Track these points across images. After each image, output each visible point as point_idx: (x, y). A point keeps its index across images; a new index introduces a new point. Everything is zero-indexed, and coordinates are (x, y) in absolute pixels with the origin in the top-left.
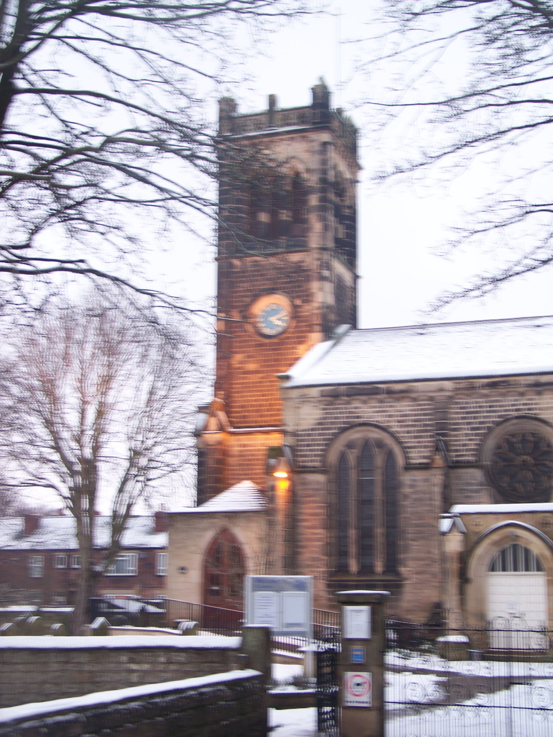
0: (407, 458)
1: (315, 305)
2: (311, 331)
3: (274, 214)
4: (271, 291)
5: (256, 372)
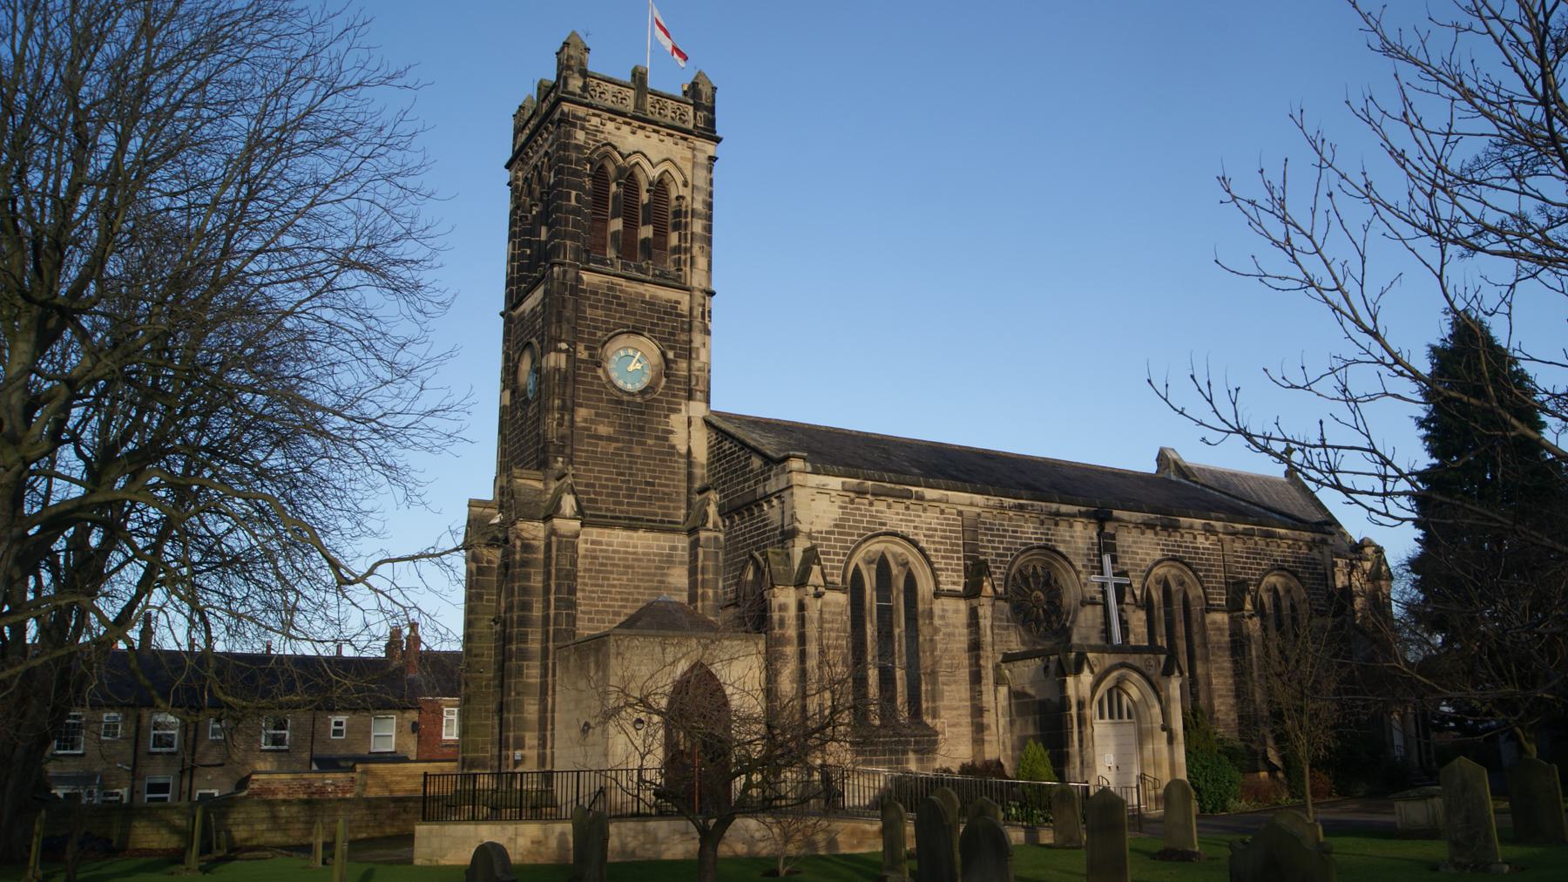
0: (937, 583)
1: (696, 364)
2: (690, 397)
3: (631, 225)
4: (636, 331)
5: (609, 439)
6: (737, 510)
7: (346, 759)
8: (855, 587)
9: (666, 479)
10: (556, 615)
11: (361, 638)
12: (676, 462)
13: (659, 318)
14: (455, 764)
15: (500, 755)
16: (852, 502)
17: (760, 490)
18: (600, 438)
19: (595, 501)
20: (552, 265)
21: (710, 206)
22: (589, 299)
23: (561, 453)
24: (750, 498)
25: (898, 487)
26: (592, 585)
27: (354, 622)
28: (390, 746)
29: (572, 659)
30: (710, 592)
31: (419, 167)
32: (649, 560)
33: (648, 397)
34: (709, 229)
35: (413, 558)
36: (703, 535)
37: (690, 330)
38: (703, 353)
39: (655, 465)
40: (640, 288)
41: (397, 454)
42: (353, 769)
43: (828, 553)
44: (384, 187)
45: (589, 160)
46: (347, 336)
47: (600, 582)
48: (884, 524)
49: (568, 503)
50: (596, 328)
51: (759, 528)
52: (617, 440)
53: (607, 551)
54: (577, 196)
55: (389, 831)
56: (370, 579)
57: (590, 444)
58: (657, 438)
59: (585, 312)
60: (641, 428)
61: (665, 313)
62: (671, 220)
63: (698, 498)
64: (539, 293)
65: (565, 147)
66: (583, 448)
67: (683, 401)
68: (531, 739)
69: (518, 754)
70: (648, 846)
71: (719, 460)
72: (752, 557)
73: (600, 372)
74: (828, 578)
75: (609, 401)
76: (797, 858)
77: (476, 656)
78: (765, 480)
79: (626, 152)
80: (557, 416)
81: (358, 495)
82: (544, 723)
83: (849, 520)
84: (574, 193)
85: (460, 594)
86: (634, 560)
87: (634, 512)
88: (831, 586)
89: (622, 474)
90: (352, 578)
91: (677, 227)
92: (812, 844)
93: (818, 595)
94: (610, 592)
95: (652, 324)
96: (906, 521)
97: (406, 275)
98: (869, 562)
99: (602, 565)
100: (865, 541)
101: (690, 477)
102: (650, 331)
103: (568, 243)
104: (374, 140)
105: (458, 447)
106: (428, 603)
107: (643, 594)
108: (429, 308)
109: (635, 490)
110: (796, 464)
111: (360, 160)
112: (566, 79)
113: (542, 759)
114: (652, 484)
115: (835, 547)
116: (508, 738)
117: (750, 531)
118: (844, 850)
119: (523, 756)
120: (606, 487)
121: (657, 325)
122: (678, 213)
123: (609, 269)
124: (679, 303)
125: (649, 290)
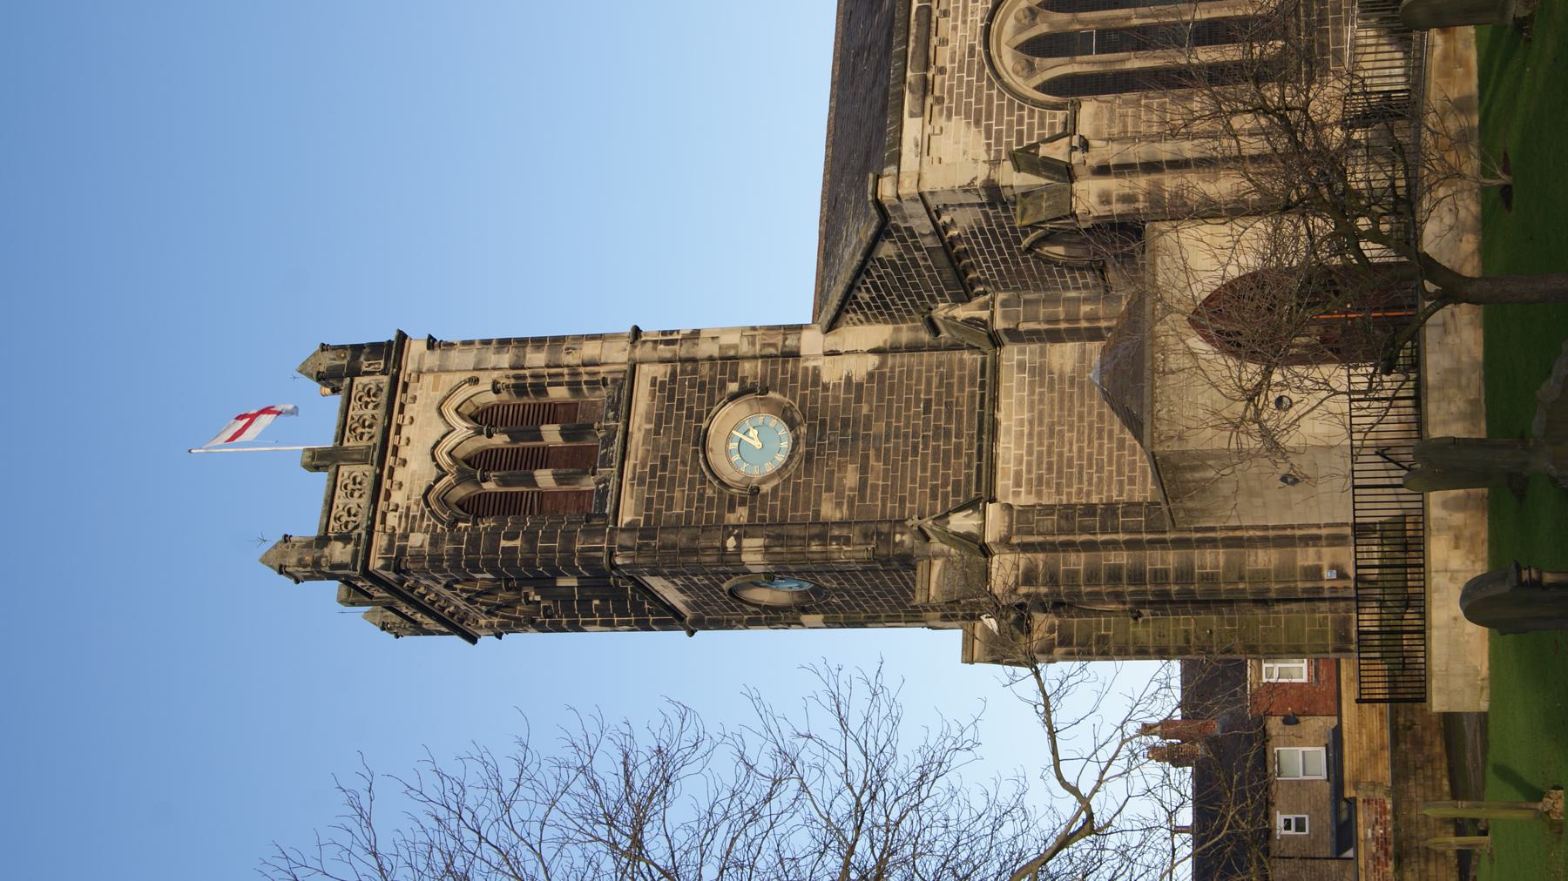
1: (745, 348)
2: (795, 355)
3: (544, 458)
4: (702, 440)
5: (864, 469)
6: (961, 274)
7: (1337, 811)
8: (1070, 89)
9: (918, 382)
10: (1126, 530)
11: (1166, 799)
12: (892, 369)
13: (680, 408)
14: (1343, 661)
15: (1332, 600)
16: (940, 100)
17: (929, 242)
18: (863, 483)
19: (957, 484)
20: (614, 567)
21: (504, 343)
22: (659, 511)
23: (886, 538)
24: (942, 258)
25: (913, 30)
26: (1080, 482)
27: (1146, 809)
28: (1319, 754)
29: (1190, 504)
30: (1085, 309)
31: (485, 764)
32: (1041, 401)
33: (798, 417)
34: (539, 342)
35: (1052, 734)
36: (999, 324)
37: (694, 360)
38: (726, 340)
39: (899, 400)
40: (637, 437)
41: (904, 766)
42: (1352, 802)
43: (1020, 133)
44: (520, 810)
45: (453, 525)
46: (739, 844)
47: (1075, 470)
48: (972, 48)
49: (962, 522)
50: (701, 497)
51: (986, 241)
52: (866, 457)
53: (1029, 464)
54: (509, 537)
55: (1438, 748)
56: (1085, 790)
57: (874, 496)
58: (859, 400)
59: (679, 516)
60: (845, 423)
61: (671, 398)
62: (530, 399)
63: (944, 334)
64: (656, 583)
65: (436, 560)
66: (880, 506)
67: (802, 364)
68: (1306, 557)
69: (1328, 574)
70: (1464, 381)
71: (886, 306)
72: (1030, 249)
73: (766, 488)
74: (1059, 130)
75: (808, 472)
76: (1484, 158)
77: (1187, 641)
78: (913, 235)
79: (435, 469)
80: (834, 546)
81: (965, 816)
82: (1284, 540)
83: (968, 104)
84: (504, 543)
85: (1100, 669)
86: (1041, 423)
87: (970, 427)
88: (1070, 128)
89: (915, 447)
90: (1084, 815)
91: (540, 390)
92: (1463, 137)
93: (1085, 145)
94: (1090, 456)
95: (689, 417)
96: (965, 14)
97: (644, 769)
98: (1031, 69)
99: (1050, 469)
100: (998, 77)
101: (914, 348)
102: (700, 420)
103: (578, 546)
104: (454, 826)
105: (890, 681)
106: (1114, 710)
107: (1091, 407)
108: (690, 735)
109: (937, 428)
110: (887, 190)
111: (484, 845)
112: (334, 567)
113: (1337, 540)
114: (928, 403)
115: (1010, 123)
116: (1305, 590)
117: (991, 254)
118: (1472, 86)
119: (1332, 568)
120: (935, 470)
121: (690, 409)
122: (520, 390)
123: (612, 485)
124: (654, 380)
125: (639, 424)
